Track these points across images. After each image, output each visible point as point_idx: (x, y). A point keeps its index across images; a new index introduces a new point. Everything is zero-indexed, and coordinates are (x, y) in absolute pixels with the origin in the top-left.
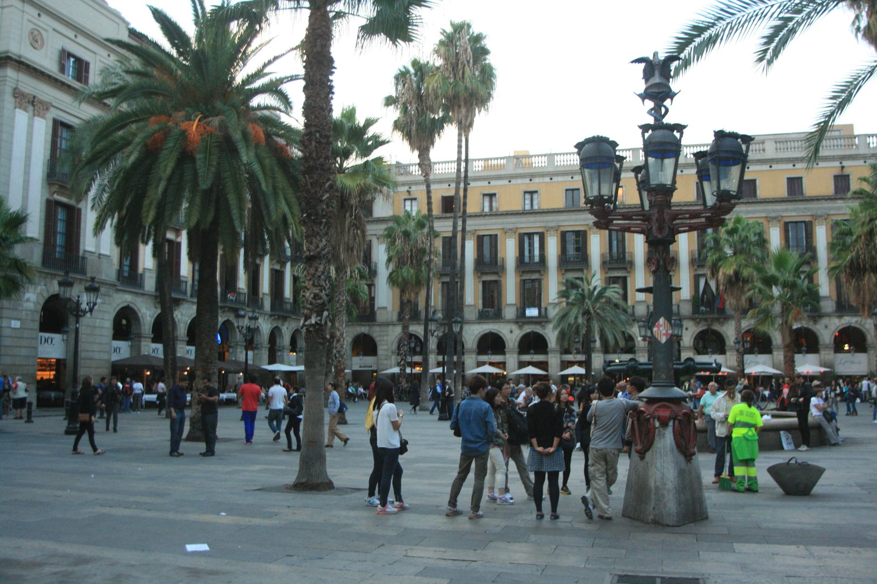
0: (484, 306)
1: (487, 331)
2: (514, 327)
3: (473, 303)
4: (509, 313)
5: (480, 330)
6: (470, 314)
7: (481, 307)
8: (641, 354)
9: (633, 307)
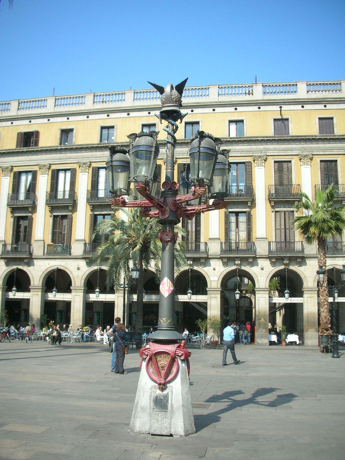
0: (53, 240)
1: (55, 268)
2: (83, 263)
3: (42, 238)
4: (77, 249)
5: (48, 266)
6: (37, 250)
7: (49, 241)
8: (213, 296)
9: (206, 244)
